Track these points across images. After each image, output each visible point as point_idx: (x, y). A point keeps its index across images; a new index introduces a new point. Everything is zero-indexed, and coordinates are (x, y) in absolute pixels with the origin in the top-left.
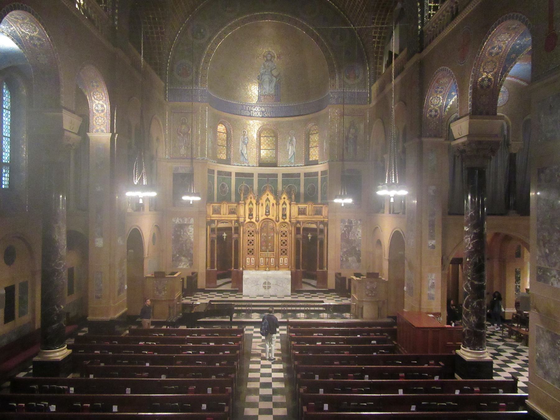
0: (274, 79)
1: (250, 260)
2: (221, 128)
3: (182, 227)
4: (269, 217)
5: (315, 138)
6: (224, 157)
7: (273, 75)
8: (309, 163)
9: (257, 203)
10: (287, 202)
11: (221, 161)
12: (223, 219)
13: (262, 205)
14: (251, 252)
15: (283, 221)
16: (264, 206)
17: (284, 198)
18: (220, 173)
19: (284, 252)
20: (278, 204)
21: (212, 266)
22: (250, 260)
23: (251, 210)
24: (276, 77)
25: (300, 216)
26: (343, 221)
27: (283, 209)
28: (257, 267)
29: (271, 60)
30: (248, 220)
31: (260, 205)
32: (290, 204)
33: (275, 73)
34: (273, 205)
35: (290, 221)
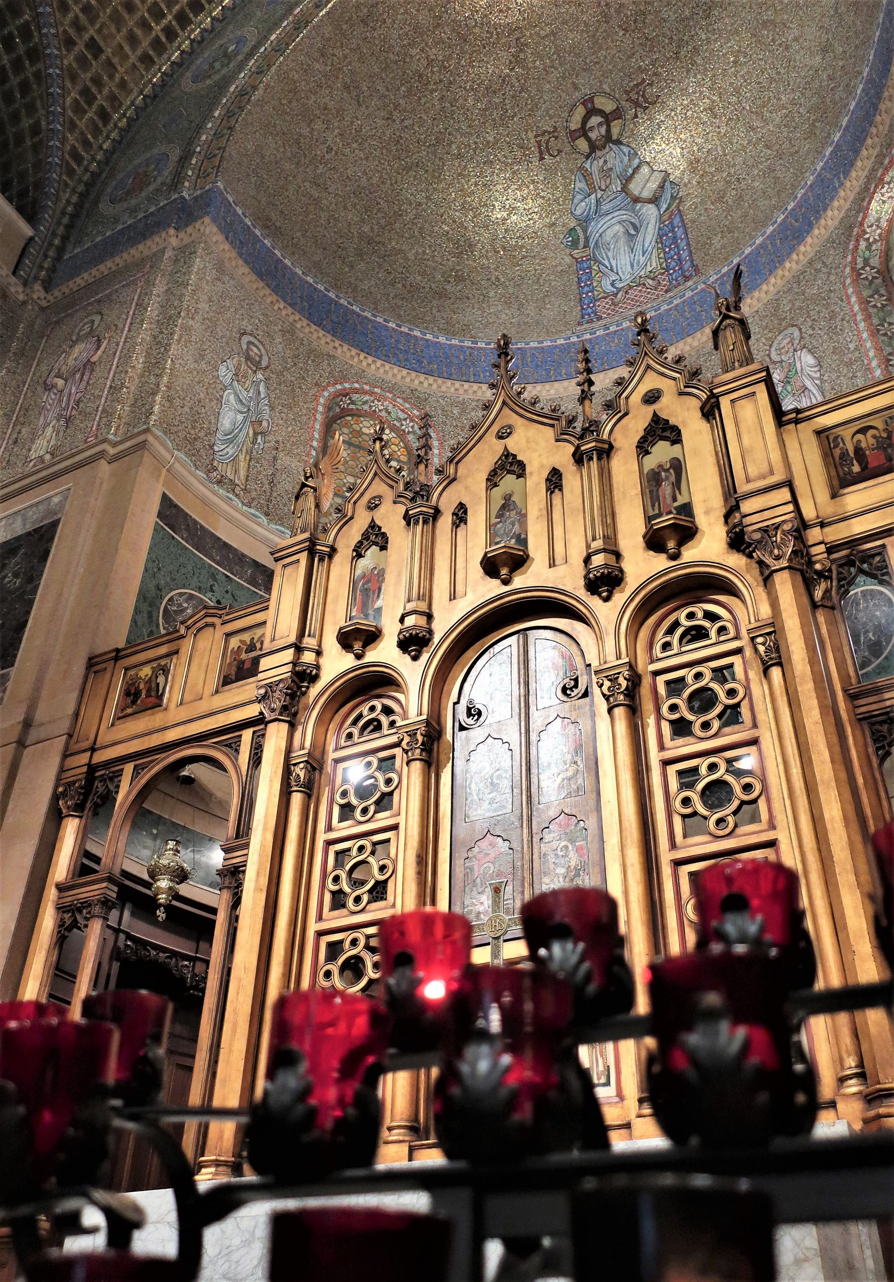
0: (650, 212)
4: (532, 578)
7: (636, 200)
10: (685, 413)
12: (172, 735)
13: (461, 516)
15: (660, 562)
16: (477, 519)
17: (652, 397)
24: (654, 200)
25: (856, 497)
27: (652, 482)
29: (608, 138)
30: (336, 663)
31: (446, 521)
32: (710, 410)
34: (555, 481)
35: (737, 541)
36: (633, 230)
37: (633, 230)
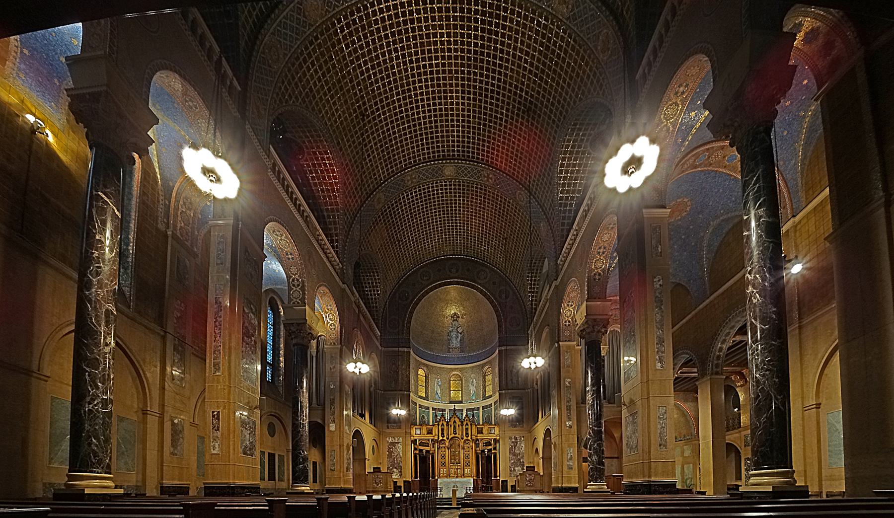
1: (443, 471)
2: (421, 372)
3: (393, 444)
5: (489, 378)
6: (424, 396)
8: (485, 398)
9: (447, 425)
11: (420, 397)
14: (444, 464)
18: (420, 406)
19: (468, 465)
20: (462, 425)
21: (416, 477)
22: (443, 471)
23: (443, 430)
26: (510, 438)
28: (448, 476)
30: (441, 438)
33: (460, 330)
36: (457, 337)
37: (457, 337)
